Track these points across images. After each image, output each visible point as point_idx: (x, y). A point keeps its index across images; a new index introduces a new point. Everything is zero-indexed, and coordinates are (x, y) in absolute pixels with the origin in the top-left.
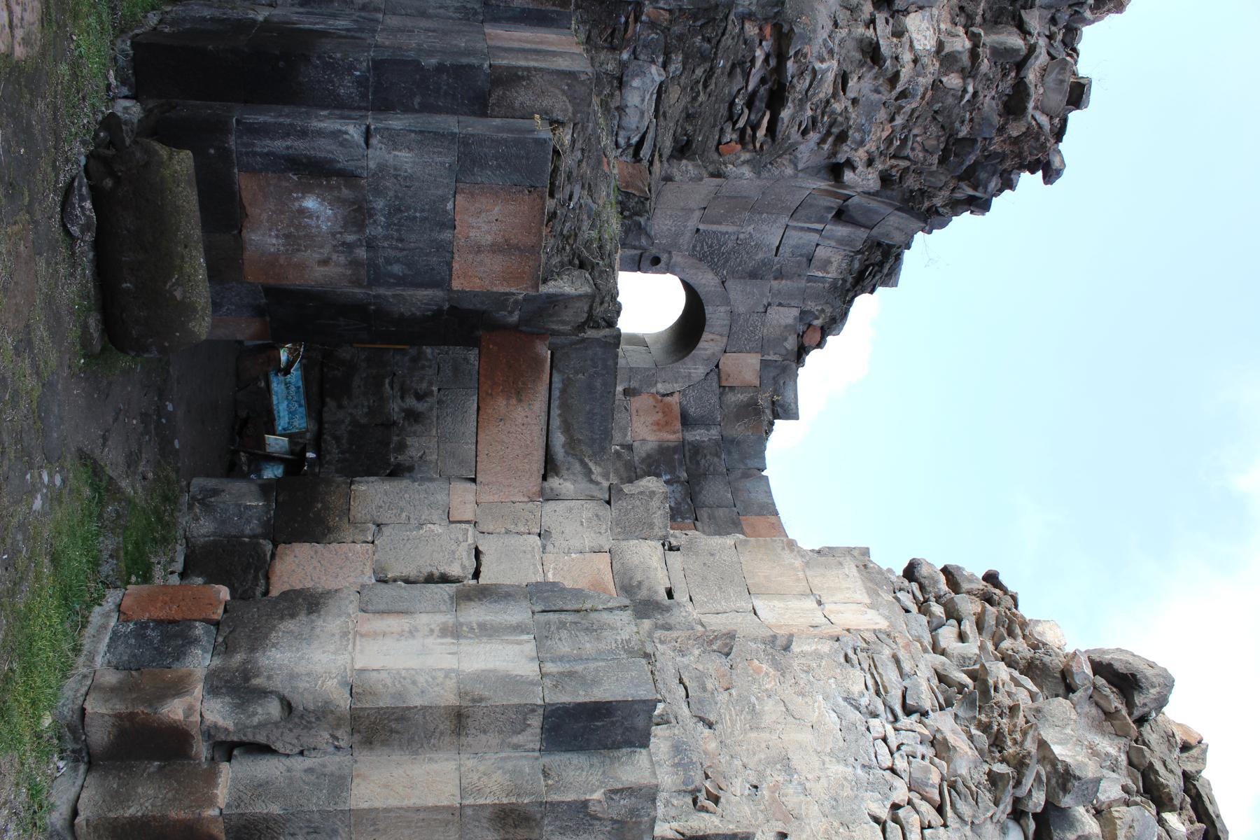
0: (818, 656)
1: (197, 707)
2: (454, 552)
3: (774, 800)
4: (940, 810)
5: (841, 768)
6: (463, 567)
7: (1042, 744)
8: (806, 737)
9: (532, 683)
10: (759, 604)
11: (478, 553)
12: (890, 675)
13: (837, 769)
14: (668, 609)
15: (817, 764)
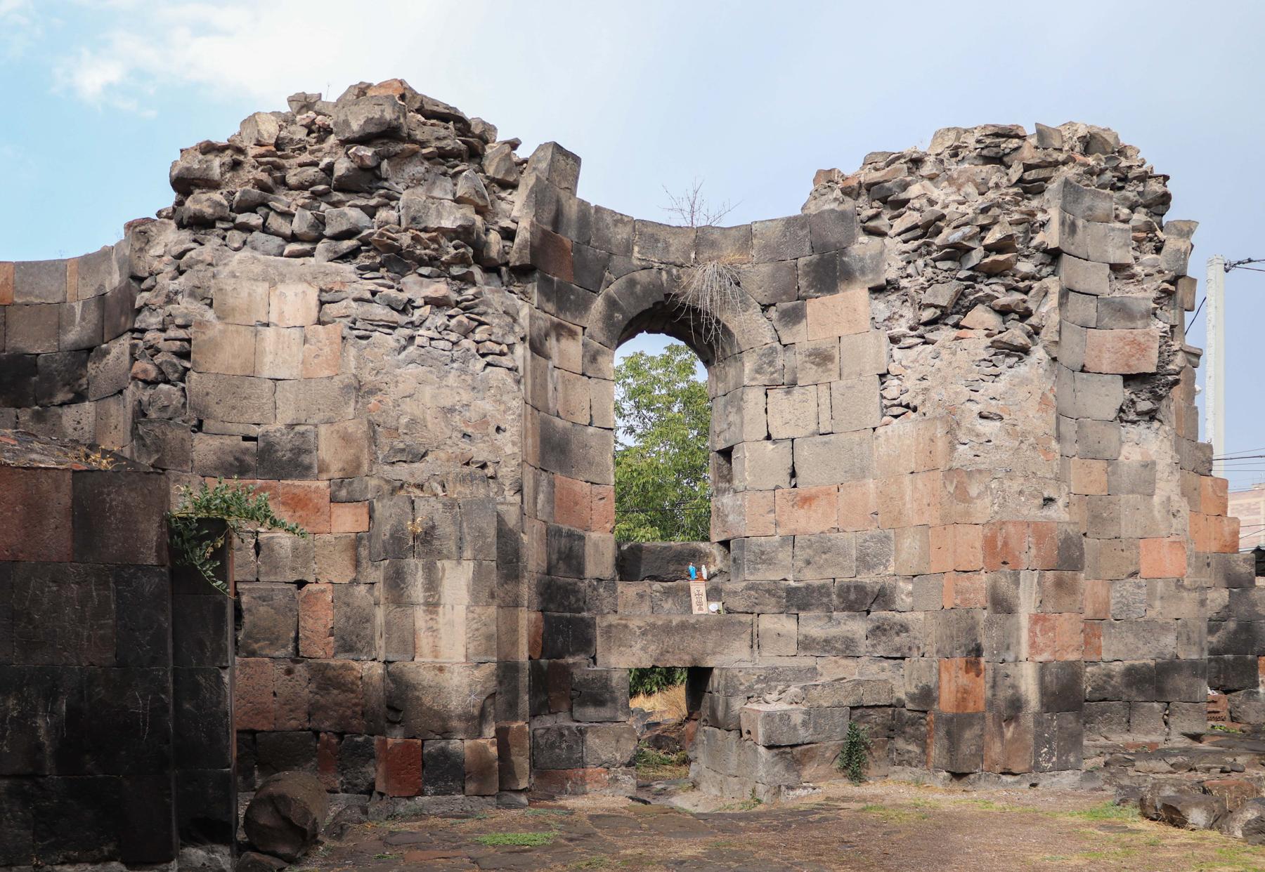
1: (488, 740)
4: (481, 323)
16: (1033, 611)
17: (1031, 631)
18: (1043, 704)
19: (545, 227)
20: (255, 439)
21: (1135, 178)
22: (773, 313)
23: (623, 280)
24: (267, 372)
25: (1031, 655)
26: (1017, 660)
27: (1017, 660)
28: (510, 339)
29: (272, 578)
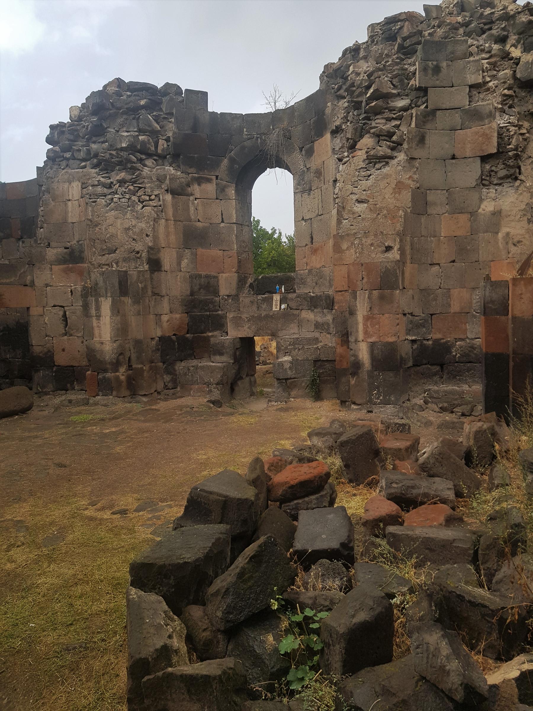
0: (93, 211)
1: (122, 373)
2: (55, 313)
3: (137, 235)
5: (128, 214)
6: (60, 311)
7: (122, 149)
8: (119, 221)
9: (114, 299)
10: (70, 220)
11: (54, 306)
12: (99, 189)
13: (128, 216)
14: (73, 250)
15: (127, 221)
16: (365, 313)
17: (364, 324)
18: (372, 365)
19: (186, 132)
20: (68, 248)
21: (497, 20)
22: (303, 152)
23: (238, 148)
24: (70, 220)
25: (365, 338)
26: (356, 341)
27: (356, 341)
28: (156, 193)
29: (76, 304)
